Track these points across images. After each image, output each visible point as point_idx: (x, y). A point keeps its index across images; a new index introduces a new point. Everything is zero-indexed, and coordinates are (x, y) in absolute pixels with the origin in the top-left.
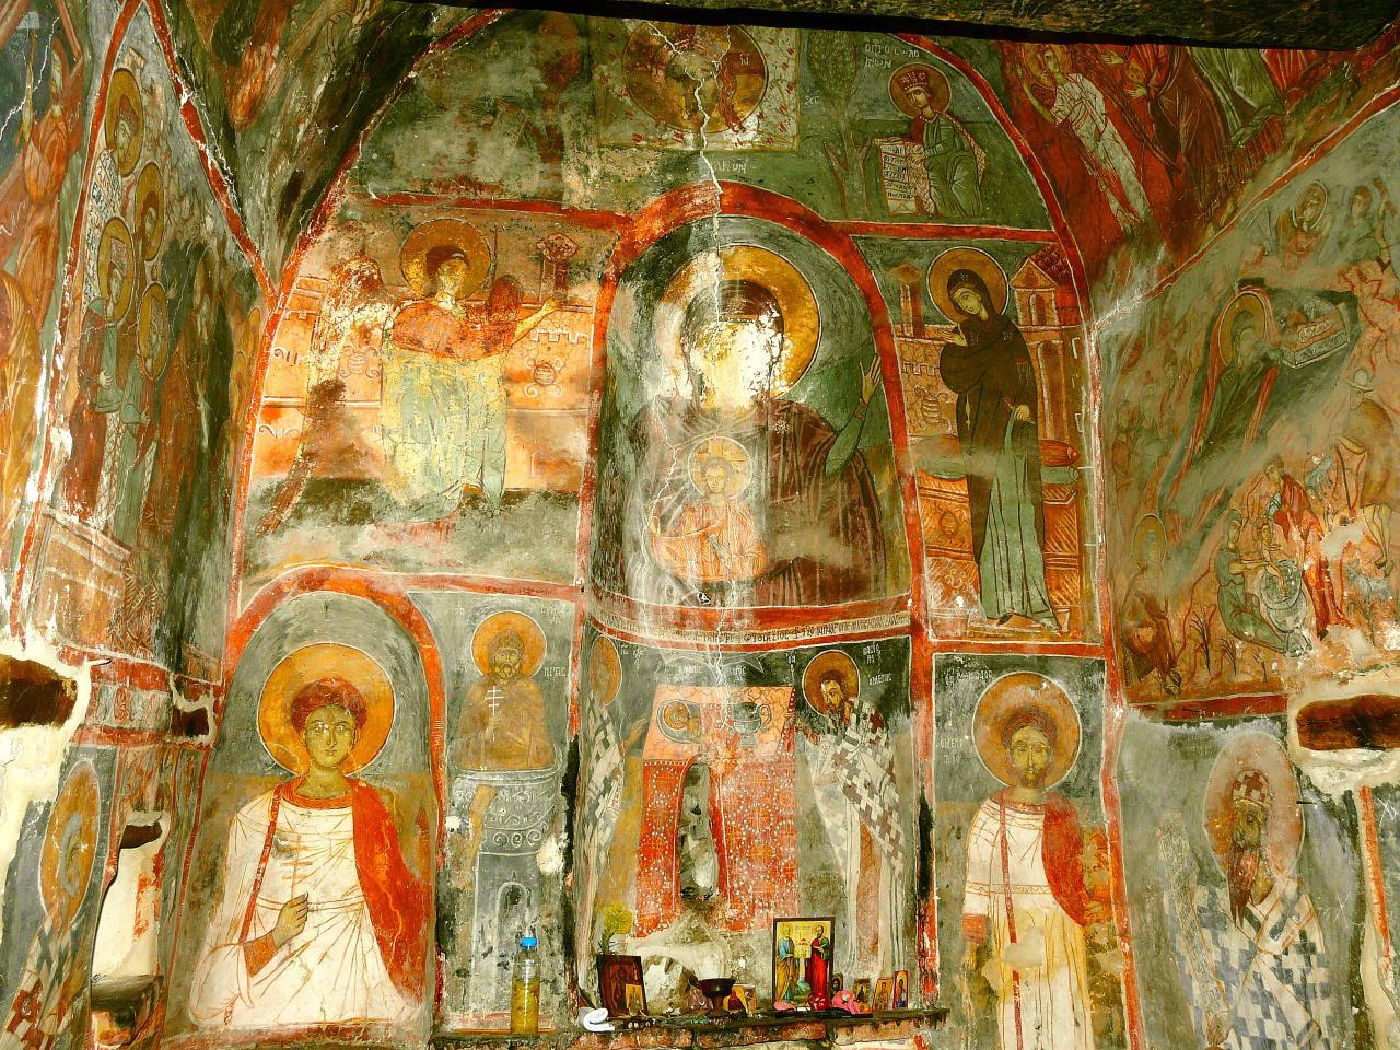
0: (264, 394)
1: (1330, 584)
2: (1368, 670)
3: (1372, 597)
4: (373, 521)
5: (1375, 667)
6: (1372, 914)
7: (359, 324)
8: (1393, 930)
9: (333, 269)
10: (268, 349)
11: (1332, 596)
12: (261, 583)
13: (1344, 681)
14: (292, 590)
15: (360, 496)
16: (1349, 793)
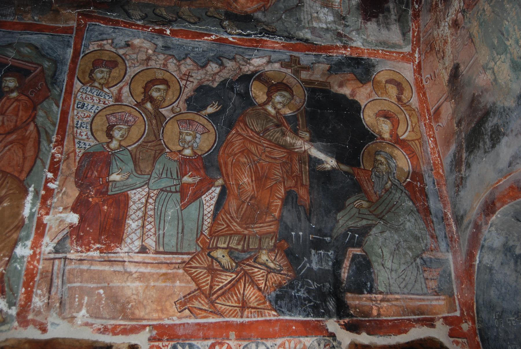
0: (431, 108)
4: (504, 134)
7: (451, 22)
9: (430, 11)
10: (422, 83)
12: (467, 227)
14: (483, 220)
15: (493, 121)
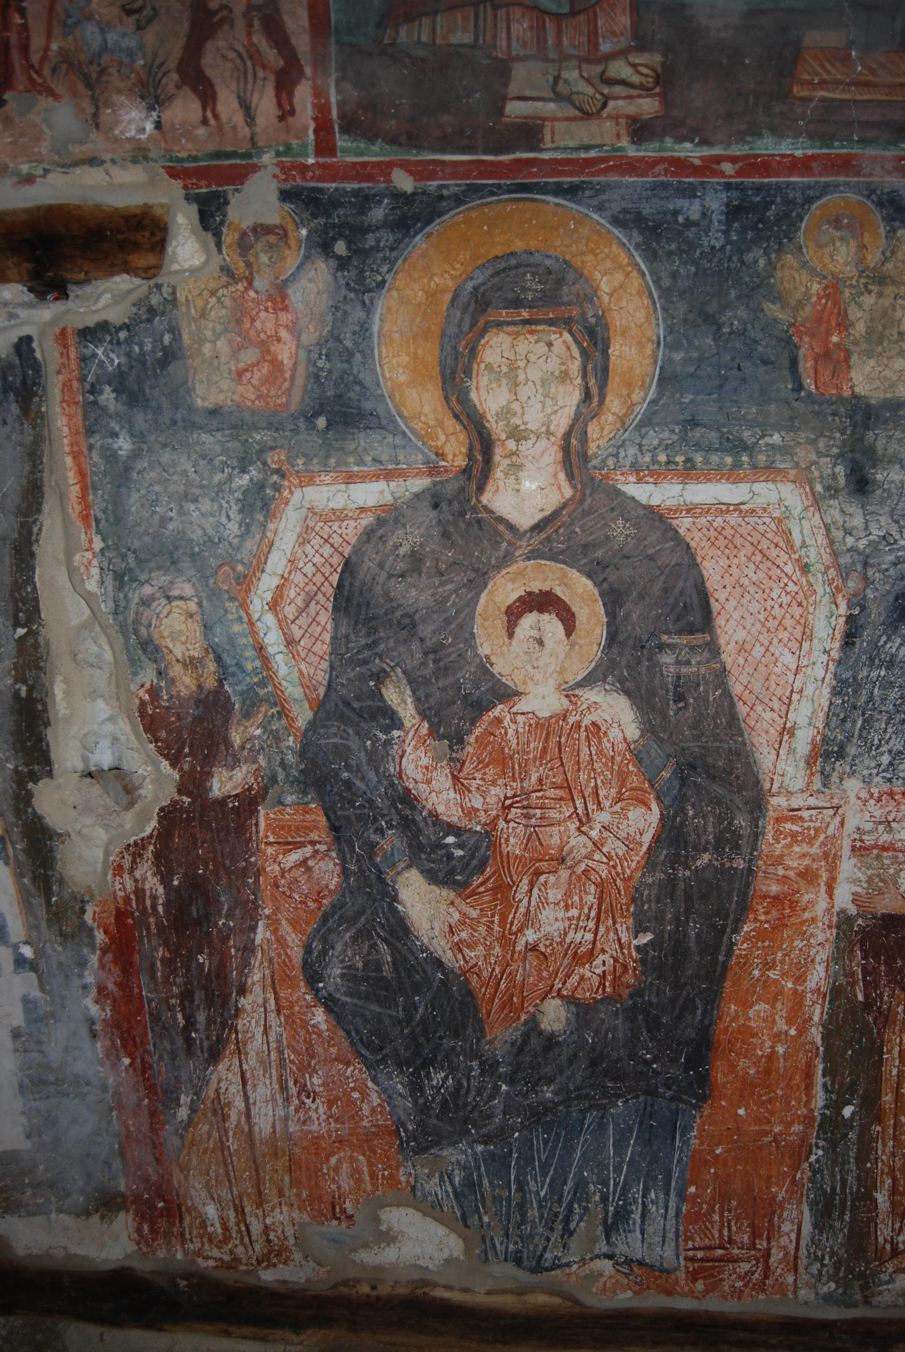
1: (25, 28)
2: (76, 164)
3: (105, 59)
5: (93, 161)
6: (62, 498)
8: (100, 515)
11: (25, 48)
13: (29, 180)
16: (27, 340)
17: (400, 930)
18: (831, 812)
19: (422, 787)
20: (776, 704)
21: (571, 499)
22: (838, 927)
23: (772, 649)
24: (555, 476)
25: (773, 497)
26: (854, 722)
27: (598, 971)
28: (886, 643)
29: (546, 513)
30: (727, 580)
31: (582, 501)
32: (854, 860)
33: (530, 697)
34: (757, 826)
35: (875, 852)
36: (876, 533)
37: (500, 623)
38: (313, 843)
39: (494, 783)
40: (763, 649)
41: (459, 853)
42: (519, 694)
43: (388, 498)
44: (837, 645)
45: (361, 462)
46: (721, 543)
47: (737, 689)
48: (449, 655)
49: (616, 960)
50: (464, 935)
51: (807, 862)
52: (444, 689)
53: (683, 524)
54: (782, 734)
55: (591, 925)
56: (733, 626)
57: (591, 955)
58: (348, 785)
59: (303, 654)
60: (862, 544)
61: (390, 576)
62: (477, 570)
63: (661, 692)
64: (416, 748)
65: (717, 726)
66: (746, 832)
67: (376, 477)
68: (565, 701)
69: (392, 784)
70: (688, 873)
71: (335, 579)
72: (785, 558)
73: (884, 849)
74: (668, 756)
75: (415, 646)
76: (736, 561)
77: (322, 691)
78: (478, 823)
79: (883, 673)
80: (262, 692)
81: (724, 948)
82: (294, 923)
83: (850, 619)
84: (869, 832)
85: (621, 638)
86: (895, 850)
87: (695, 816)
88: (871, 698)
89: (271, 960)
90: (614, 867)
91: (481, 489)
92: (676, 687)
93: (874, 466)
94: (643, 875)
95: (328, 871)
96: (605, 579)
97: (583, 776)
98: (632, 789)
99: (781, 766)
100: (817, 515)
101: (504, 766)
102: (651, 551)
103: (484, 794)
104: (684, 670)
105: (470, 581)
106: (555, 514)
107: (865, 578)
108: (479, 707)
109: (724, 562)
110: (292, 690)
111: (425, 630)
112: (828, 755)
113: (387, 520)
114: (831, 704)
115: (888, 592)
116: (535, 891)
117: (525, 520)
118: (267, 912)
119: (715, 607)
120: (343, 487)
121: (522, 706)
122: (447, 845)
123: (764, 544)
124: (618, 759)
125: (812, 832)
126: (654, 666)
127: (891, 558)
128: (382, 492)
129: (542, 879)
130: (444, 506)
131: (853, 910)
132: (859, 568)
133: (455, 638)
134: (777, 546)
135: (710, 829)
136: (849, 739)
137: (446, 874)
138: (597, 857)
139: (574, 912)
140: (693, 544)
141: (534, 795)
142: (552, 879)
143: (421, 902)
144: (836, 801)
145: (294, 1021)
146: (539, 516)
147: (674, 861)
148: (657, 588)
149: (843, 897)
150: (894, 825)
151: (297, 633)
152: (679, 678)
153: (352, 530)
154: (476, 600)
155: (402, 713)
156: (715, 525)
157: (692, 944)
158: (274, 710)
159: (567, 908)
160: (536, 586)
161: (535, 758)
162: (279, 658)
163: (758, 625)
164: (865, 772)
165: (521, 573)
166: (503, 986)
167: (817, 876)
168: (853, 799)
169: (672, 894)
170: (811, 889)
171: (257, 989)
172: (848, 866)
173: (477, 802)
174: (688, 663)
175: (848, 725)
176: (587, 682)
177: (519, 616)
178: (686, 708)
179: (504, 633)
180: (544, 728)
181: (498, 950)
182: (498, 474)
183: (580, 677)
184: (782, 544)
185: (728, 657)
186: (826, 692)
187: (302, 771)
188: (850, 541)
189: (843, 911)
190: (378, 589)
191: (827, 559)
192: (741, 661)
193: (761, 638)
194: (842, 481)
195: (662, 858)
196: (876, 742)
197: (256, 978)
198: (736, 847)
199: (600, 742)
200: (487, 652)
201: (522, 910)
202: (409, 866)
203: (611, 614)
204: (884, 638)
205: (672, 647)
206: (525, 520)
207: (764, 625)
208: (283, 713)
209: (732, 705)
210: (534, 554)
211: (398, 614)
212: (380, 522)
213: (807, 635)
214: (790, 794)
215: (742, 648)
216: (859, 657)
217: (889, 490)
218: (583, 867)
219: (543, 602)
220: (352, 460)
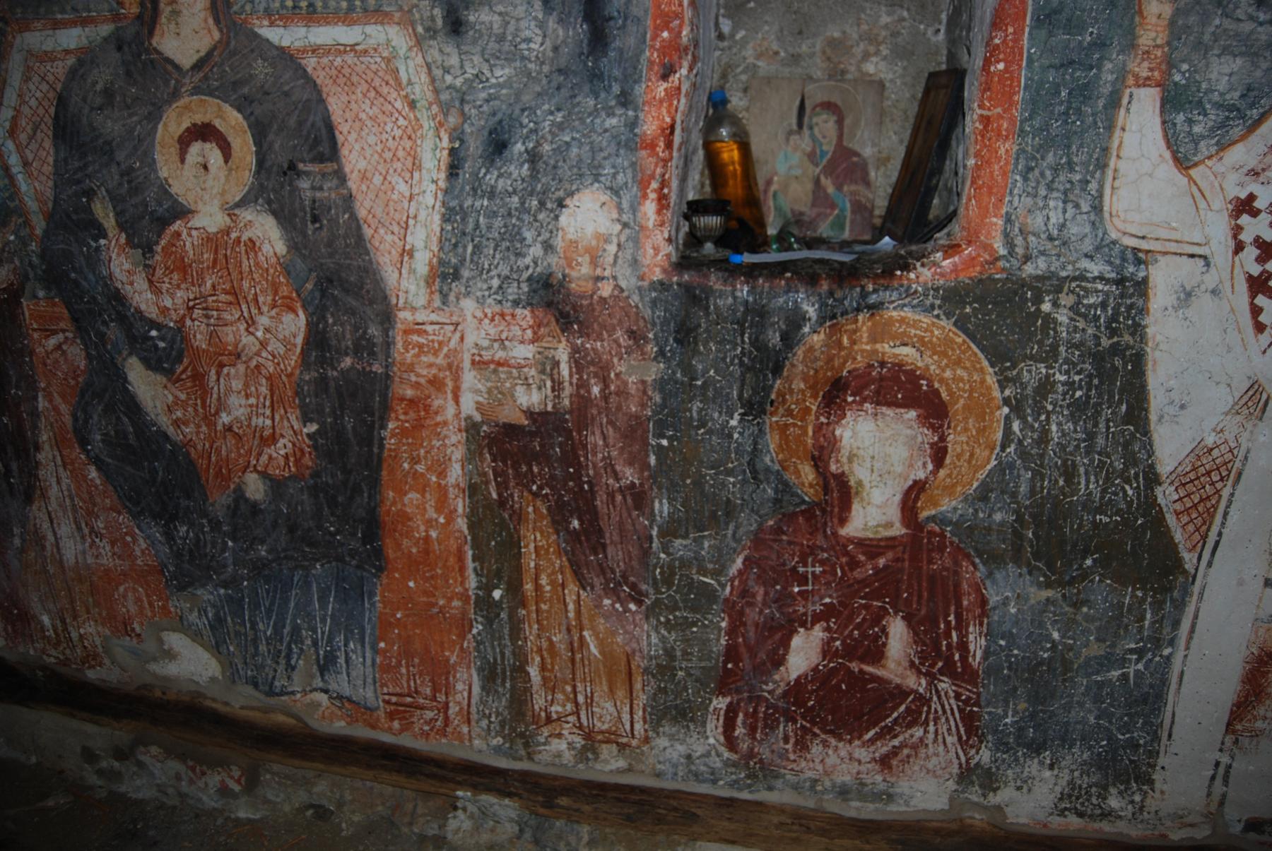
17: (133, 407)
18: (451, 328)
19: (128, 287)
20: (396, 229)
21: (220, 42)
22: (467, 431)
23: (389, 178)
24: (206, 21)
25: (382, 38)
26: (465, 247)
27: (282, 452)
28: (485, 175)
29: (202, 54)
30: (348, 115)
31: (228, 43)
32: (473, 373)
33: (200, 215)
34: (387, 336)
35: (492, 366)
36: (471, 71)
37: (174, 150)
38: (63, 331)
39: (178, 287)
40: (381, 178)
41: (162, 345)
42: (192, 212)
43: (85, 42)
44: (443, 176)
45: (63, 11)
46: (341, 80)
47: (362, 213)
48: (138, 177)
49: (294, 445)
50: (179, 414)
51: (434, 371)
52: (135, 206)
53: (310, 63)
54: (402, 255)
55: (268, 412)
56: (356, 156)
57: (273, 439)
58: (76, 284)
59: (35, 173)
60: (459, 82)
61: (92, 109)
62: (154, 104)
63: (301, 214)
64: (119, 255)
65: (347, 246)
66: (379, 340)
67: (73, 24)
68: (227, 219)
69: (106, 285)
70: (335, 373)
71: (52, 110)
72: (394, 95)
73: (499, 364)
74: (311, 270)
75: (114, 169)
76: (354, 97)
77: (50, 205)
78: (171, 320)
79: (486, 203)
80: (12, 205)
81: (376, 442)
82: (63, 396)
83: (453, 152)
84: (487, 349)
85: (268, 164)
86: (509, 366)
87: (334, 324)
88: (477, 226)
89: (51, 425)
90: (278, 364)
91: (151, 33)
92: (313, 209)
93: (467, 8)
94: (301, 372)
95: (77, 354)
96: (252, 113)
97: (246, 284)
98: (283, 297)
99: (404, 284)
100: (420, 55)
101: (185, 273)
102: (286, 88)
103: (172, 296)
104: (318, 195)
105: (150, 113)
106: (209, 54)
107: (463, 113)
108: (162, 223)
109: (345, 98)
110: (32, 205)
111: (120, 156)
112: (445, 276)
113: (85, 59)
114: (442, 229)
115: (483, 127)
116: (222, 380)
117: (186, 61)
118: (43, 385)
119: (340, 139)
120: (50, 32)
121: (196, 222)
122: (152, 338)
123: (377, 82)
124: (271, 271)
125: (436, 345)
126: (295, 190)
127: (483, 95)
128: (80, 36)
129: (225, 370)
130: (126, 49)
131: (478, 418)
132: (457, 104)
133: (141, 162)
134: (387, 83)
135: (348, 336)
136: (463, 261)
137: (155, 362)
138: (264, 354)
139: (252, 401)
140: (319, 82)
141: (210, 299)
142: (233, 371)
143: (143, 383)
144: (455, 319)
145: (79, 477)
146: (196, 57)
147: (322, 361)
148: (292, 122)
149: (468, 404)
150: (507, 343)
151: (30, 157)
152: (314, 201)
153: (60, 69)
154: (155, 128)
155: (106, 225)
156: (336, 64)
157: (350, 436)
158: (21, 220)
159: (247, 396)
160: (199, 118)
161: (208, 268)
162: (20, 177)
163: (376, 156)
164: (479, 294)
165: (187, 108)
166: (213, 459)
167: (445, 385)
168: (469, 318)
169: (326, 390)
170: (440, 395)
171: (47, 447)
172: (469, 378)
173: (168, 303)
174: (321, 189)
175: (460, 250)
176: (242, 203)
177: (188, 145)
178: (321, 228)
179: (177, 158)
180: (213, 242)
181: (204, 428)
182: (164, 20)
183: (237, 199)
184: (391, 82)
185: (353, 184)
186: (437, 218)
187: (44, 271)
188: (449, 78)
189: (469, 418)
190: (84, 120)
191: (430, 96)
192: (364, 188)
193: (380, 168)
194: (440, 22)
195: (313, 358)
196: (486, 266)
197: (45, 438)
198: (372, 354)
199: (256, 253)
200: (166, 175)
201: (215, 396)
202: (130, 354)
203: (258, 143)
204: (483, 171)
205: (307, 174)
206: (186, 61)
207: (381, 156)
208: (27, 223)
209: (359, 228)
210: (196, 91)
211: (101, 141)
212: (81, 62)
213: (416, 165)
214: (414, 309)
215: (364, 177)
216: (462, 189)
217: (480, 31)
218: (254, 363)
219: (204, 132)
220: (56, 9)
